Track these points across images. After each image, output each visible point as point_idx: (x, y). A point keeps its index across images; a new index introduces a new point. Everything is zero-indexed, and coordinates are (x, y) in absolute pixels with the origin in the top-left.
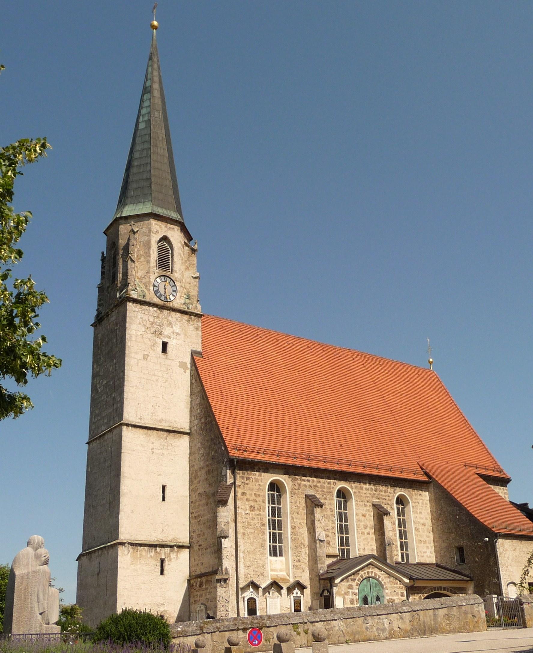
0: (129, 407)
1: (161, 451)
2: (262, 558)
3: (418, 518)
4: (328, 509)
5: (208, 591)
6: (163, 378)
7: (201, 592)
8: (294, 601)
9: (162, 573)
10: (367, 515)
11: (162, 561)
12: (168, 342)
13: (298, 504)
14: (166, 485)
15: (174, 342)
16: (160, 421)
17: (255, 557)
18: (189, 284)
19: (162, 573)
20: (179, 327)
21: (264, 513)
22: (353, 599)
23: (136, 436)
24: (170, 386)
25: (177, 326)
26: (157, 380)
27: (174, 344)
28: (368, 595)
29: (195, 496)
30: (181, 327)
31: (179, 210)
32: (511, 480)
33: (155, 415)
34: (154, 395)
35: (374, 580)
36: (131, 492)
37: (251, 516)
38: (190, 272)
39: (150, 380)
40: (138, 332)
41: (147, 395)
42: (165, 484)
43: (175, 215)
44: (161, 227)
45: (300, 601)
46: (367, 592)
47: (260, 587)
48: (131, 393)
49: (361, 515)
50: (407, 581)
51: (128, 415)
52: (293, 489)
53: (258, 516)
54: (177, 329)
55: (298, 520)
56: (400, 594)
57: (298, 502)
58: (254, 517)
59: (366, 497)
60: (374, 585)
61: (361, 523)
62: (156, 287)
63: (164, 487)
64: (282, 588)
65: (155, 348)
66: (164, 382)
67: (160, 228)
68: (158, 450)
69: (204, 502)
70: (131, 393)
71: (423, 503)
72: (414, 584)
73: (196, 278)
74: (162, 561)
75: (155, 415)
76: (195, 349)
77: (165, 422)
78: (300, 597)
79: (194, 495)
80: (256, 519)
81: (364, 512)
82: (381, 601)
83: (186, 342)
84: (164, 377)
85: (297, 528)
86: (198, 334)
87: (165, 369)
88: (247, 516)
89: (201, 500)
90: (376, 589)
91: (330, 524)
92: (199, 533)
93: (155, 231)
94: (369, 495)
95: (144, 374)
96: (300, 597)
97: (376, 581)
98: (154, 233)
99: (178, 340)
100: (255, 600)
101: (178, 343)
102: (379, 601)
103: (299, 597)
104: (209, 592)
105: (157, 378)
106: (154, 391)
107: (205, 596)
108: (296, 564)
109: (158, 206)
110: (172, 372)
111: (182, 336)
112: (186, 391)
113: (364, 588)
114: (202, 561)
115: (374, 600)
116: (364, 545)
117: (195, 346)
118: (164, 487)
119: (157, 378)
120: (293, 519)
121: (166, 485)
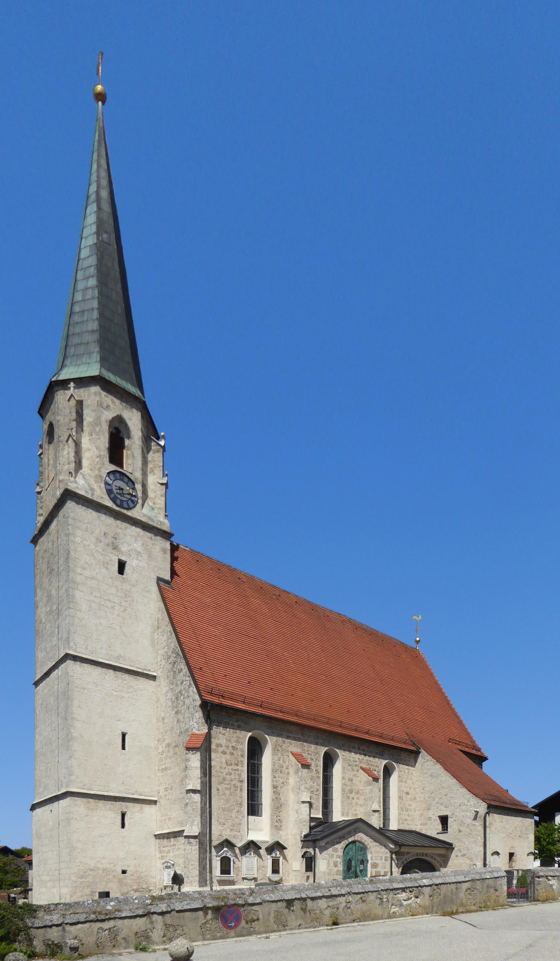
0: (76, 635)
1: (119, 693)
2: (239, 816)
3: (403, 786)
4: (314, 770)
5: (176, 847)
6: (120, 605)
7: (169, 848)
8: (272, 861)
9: (123, 826)
10: (354, 779)
11: (123, 815)
12: (126, 562)
13: (281, 762)
14: (127, 733)
15: (134, 562)
16: (119, 658)
17: (230, 815)
18: (155, 492)
19: (123, 826)
20: (140, 544)
21: (242, 768)
22: (337, 862)
23: (87, 672)
24: (130, 618)
25: (138, 542)
26: (113, 607)
27: (134, 565)
28: (352, 859)
29: (162, 747)
30: (143, 544)
31: (140, 385)
32: (488, 759)
33: (111, 650)
34: (109, 625)
35: (360, 844)
36: (81, 736)
37: (227, 771)
38: (155, 477)
39: (103, 605)
40: (86, 541)
41: (100, 623)
42: (125, 732)
43: (133, 390)
44: (113, 402)
45: (279, 861)
46: (351, 856)
47: (235, 846)
48: (78, 618)
49: (347, 779)
50: (392, 846)
51: (76, 645)
52: (276, 746)
53: (235, 771)
54: (138, 546)
55: (280, 779)
56: (384, 858)
57: (282, 759)
58: (230, 772)
59: (354, 761)
60: (360, 849)
61: (347, 788)
62: (109, 485)
63: (124, 735)
64: (260, 848)
65: (109, 567)
66: (122, 612)
67: (112, 403)
68: (116, 691)
69: (171, 754)
70: (78, 618)
71: (408, 773)
72: (400, 850)
73: (162, 484)
74: (123, 815)
75: (111, 650)
76: (161, 576)
77: (124, 660)
78: (279, 857)
79: (161, 746)
80: (233, 774)
81: (351, 777)
82: (365, 864)
83: (150, 566)
84: (122, 604)
85: (279, 787)
86: (166, 557)
87: (122, 595)
88: (222, 770)
89: (169, 751)
90: (361, 853)
91: (316, 785)
92: (167, 786)
93: (106, 405)
94: (357, 760)
95: (95, 597)
96: (279, 857)
97: (362, 845)
98: (104, 409)
99: (140, 561)
100: (229, 859)
101: (140, 565)
102: (363, 864)
103: (278, 857)
104: (177, 849)
105: (113, 604)
106: (109, 621)
107: (173, 852)
108: (277, 824)
109: (109, 370)
110: (133, 601)
111: (145, 556)
112: (151, 626)
113: (349, 851)
114: (170, 816)
115: (359, 863)
116: (348, 809)
117: (162, 573)
118: (124, 735)
119: (113, 604)
120: (275, 778)
121: (127, 733)
